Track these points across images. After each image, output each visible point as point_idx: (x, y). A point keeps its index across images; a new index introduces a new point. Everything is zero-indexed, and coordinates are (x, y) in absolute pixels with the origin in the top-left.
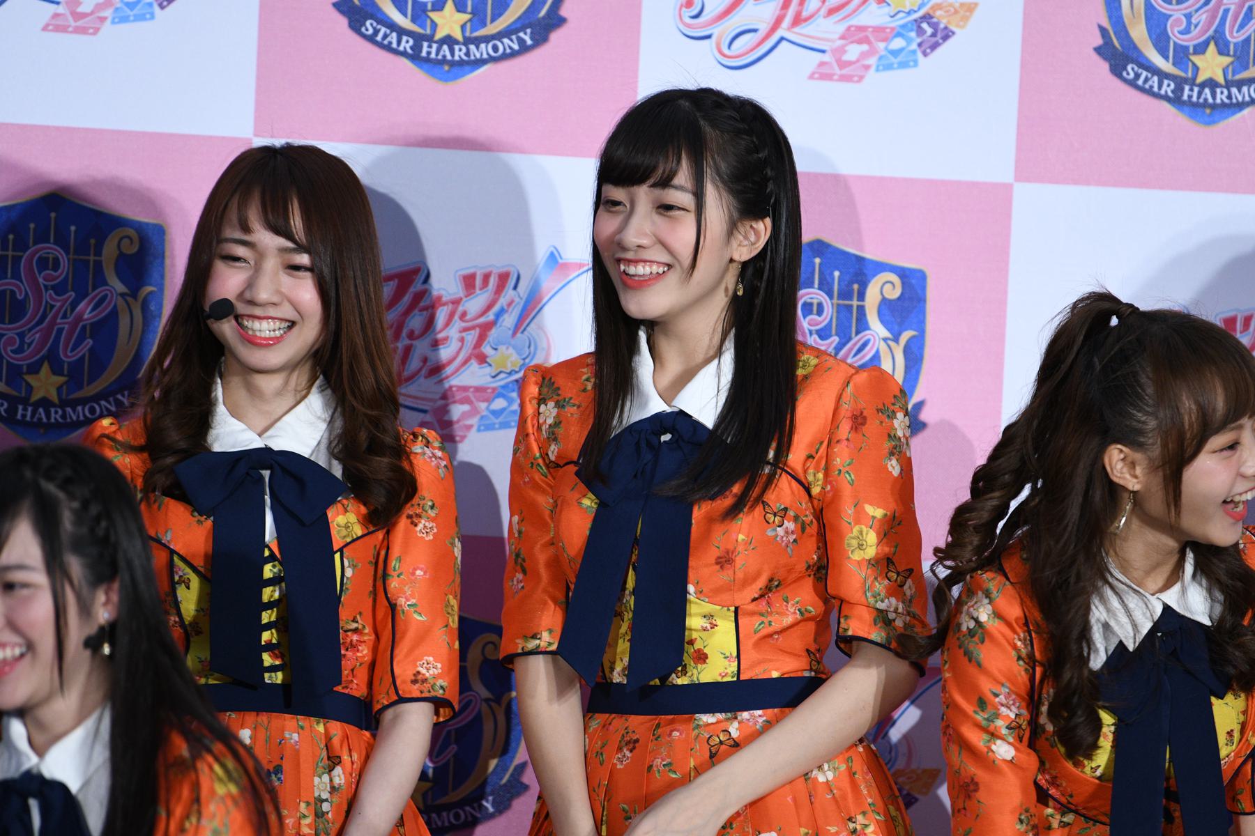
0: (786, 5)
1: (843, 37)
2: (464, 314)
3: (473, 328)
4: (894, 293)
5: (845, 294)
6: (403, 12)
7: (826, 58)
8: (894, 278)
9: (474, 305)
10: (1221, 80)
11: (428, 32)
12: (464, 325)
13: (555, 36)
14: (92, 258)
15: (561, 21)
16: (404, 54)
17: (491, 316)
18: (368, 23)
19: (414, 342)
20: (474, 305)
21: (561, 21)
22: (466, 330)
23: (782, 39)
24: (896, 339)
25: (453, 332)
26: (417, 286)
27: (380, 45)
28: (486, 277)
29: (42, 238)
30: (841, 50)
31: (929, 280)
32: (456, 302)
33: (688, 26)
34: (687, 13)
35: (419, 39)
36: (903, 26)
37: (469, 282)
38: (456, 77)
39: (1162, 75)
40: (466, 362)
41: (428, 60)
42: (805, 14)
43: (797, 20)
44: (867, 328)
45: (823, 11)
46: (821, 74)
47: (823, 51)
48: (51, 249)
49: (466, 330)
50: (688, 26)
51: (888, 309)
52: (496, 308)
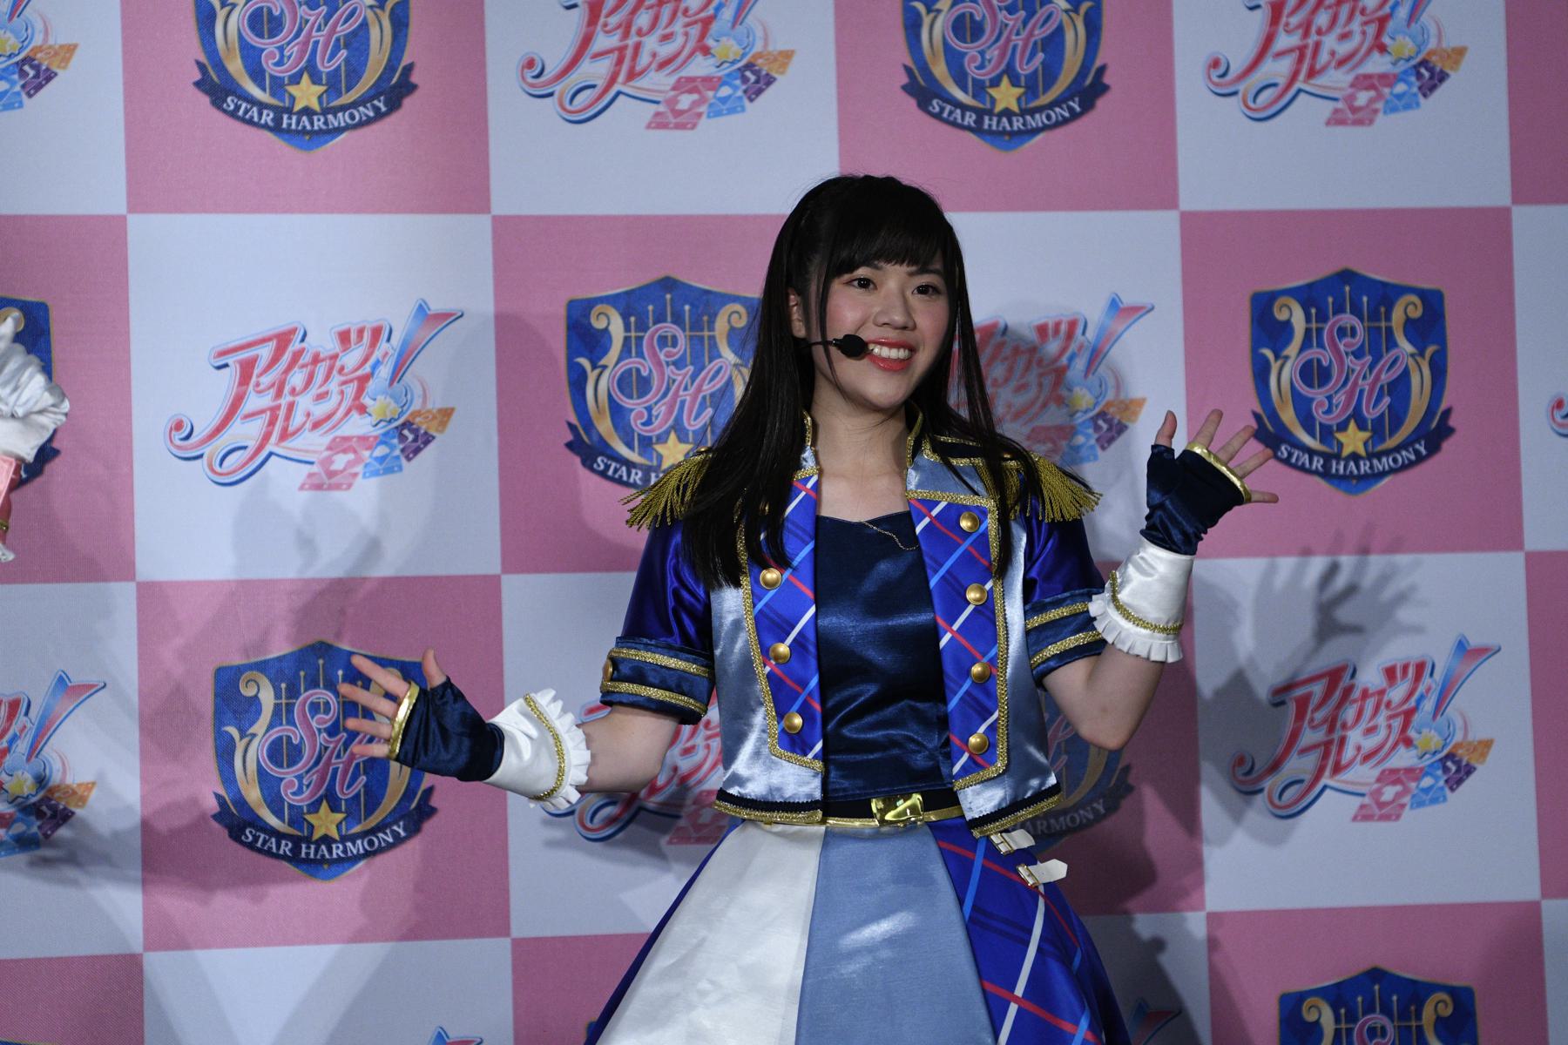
0: (620, 62)
1: (674, 88)
2: (342, 369)
3: (351, 381)
4: (1416, 313)
5: (1374, 315)
6: (964, 89)
7: (661, 108)
8: (1414, 298)
9: (351, 359)
10: (1015, 108)
11: (988, 106)
12: (343, 378)
13: (1101, 103)
14: (633, 334)
15: (1106, 88)
16: (266, 126)
17: (367, 368)
18: (935, 102)
19: (1000, 390)
20: (351, 359)
21: (1106, 88)
22: (345, 383)
23: (619, 93)
24: (1422, 354)
25: (333, 386)
26: (295, 345)
27: (947, 122)
28: (361, 332)
29: (1339, 309)
30: (1352, 98)
31: (1446, 302)
32: (334, 357)
33: (1216, 85)
34: (529, 74)
35: (980, 114)
36: (729, 75)
37: (1042, 330)
38: (1016, 147)
39: (964, 108)
40: (348, 412)
41: (289, 130)
42: (1318, 67)
43: (1312, 73)
44: (1395, 345)
45: (654, 66)
46: (1336, 120)
47: (1335, 99)
48: (1348, 319)
49: (345, 383)
50: (532, 86)
51: (1411, 326)
52: (1067, 354)
